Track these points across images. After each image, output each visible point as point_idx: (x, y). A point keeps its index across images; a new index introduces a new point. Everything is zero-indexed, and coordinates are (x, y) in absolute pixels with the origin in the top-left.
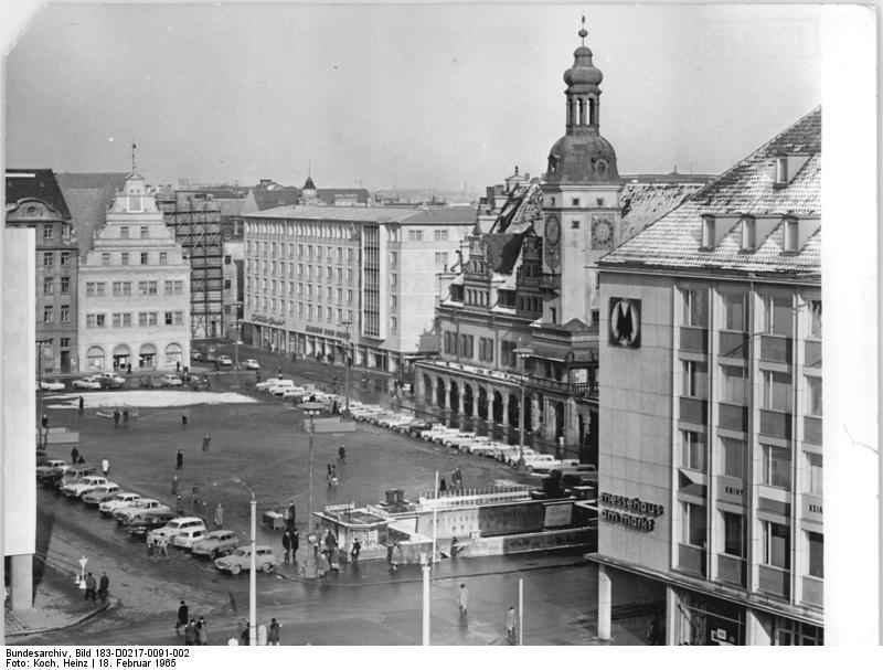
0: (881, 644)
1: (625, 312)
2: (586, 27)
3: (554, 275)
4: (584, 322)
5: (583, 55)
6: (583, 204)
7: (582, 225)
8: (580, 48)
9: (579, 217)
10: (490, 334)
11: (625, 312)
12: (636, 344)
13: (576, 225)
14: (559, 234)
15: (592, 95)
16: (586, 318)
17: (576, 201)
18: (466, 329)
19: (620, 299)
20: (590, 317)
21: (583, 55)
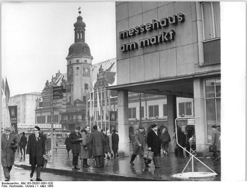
0: (246, 181)
3: (70, 85)
4: (81, 100)
5: (80, 19)
6: (80, 62)
7: (80, 68)
8: (79, 17)
9: (79, 66)
15: (82, 30)
16: (81, 98)
17: (78, 61)
18: (43, 114)
21: (80, 19)
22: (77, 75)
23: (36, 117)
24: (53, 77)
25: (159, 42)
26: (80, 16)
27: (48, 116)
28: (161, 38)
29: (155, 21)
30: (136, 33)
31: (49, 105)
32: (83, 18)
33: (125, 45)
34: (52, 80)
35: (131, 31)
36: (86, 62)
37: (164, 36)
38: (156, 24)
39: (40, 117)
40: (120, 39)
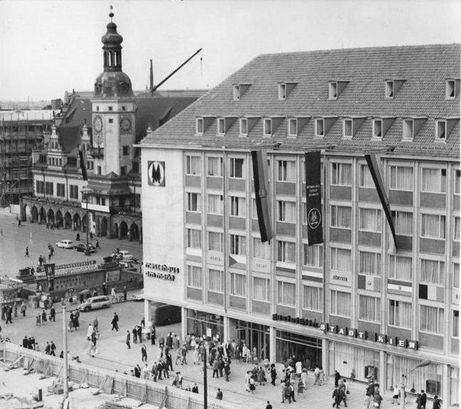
1: (156, 169)
2: (113, 11)
5: (112, 28)
10: (63, 181)
11: (156, 169)
12: (163, 185)
13: (111, 121)
14: (102, 127)
17: (111, 108)
18: (48, 179)
19: (153, 162)
21: (112, 28)
22: (111, 131)
25: (166, 278)
27: (58, 185)
39: (43, 183)
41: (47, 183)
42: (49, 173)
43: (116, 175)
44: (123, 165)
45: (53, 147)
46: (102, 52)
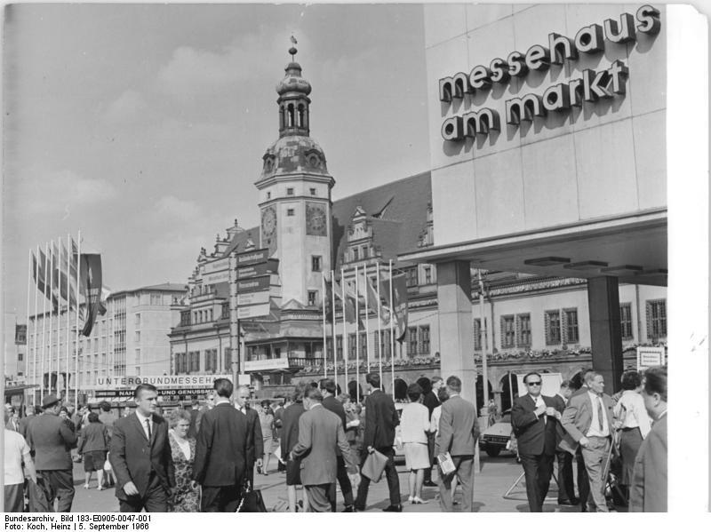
2: (295, 46)
4: (301, 302)
6: (297, 194)
7: (295, 212)
13: (291, 212)
17: (290, 191)
20: (306, 296)
23: (173, 356)
24: (218, 238)
26: (296, 61)
28: (580, 89)
29: (556, 36)
30: (493, 78)
31: (209, 319)
32: (302, 67)
33: (460, 121)
34: (216, 246)
35: (479, 73)
36: (313, 193)
37: (591, 83)
38: (560, 47)
39: (184, 354)
40: (442, 100)
41: (192, 353)
42: (193, 336)
43: (299, 305)
44: (312, 288)
45: (200, 295)
46: (277, 107)
